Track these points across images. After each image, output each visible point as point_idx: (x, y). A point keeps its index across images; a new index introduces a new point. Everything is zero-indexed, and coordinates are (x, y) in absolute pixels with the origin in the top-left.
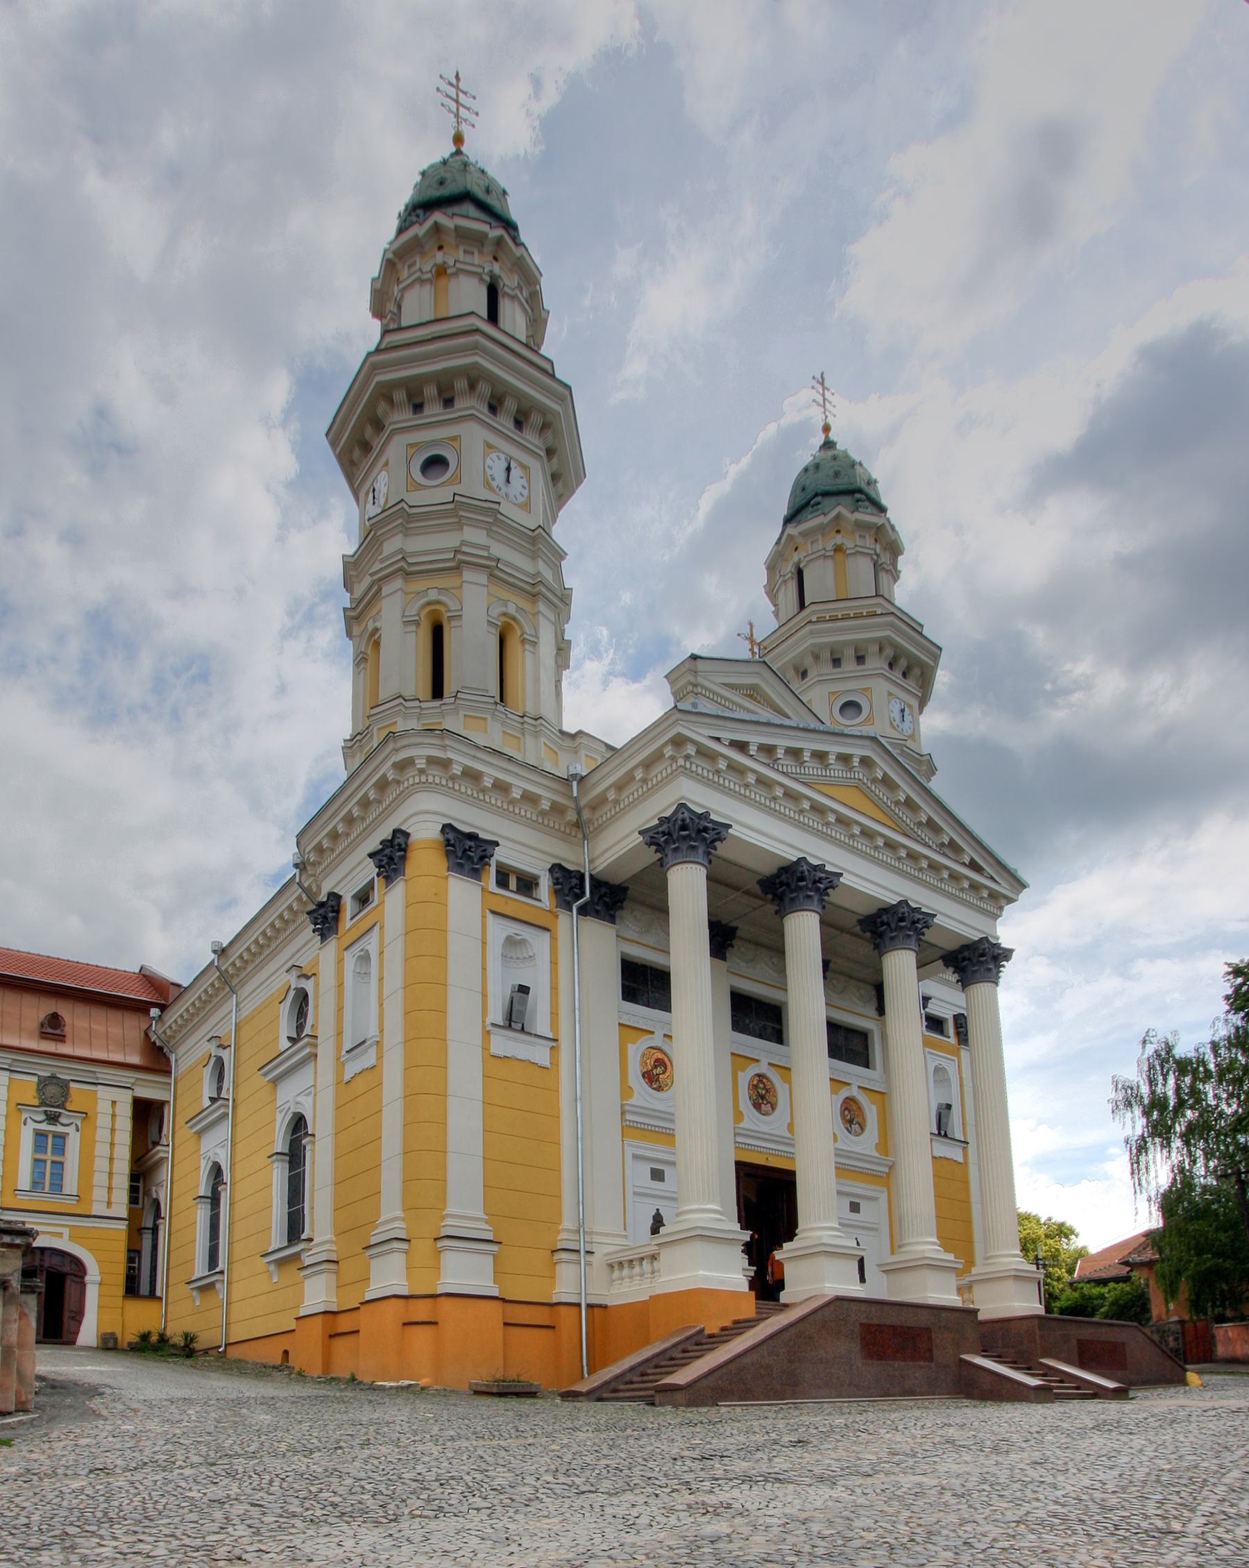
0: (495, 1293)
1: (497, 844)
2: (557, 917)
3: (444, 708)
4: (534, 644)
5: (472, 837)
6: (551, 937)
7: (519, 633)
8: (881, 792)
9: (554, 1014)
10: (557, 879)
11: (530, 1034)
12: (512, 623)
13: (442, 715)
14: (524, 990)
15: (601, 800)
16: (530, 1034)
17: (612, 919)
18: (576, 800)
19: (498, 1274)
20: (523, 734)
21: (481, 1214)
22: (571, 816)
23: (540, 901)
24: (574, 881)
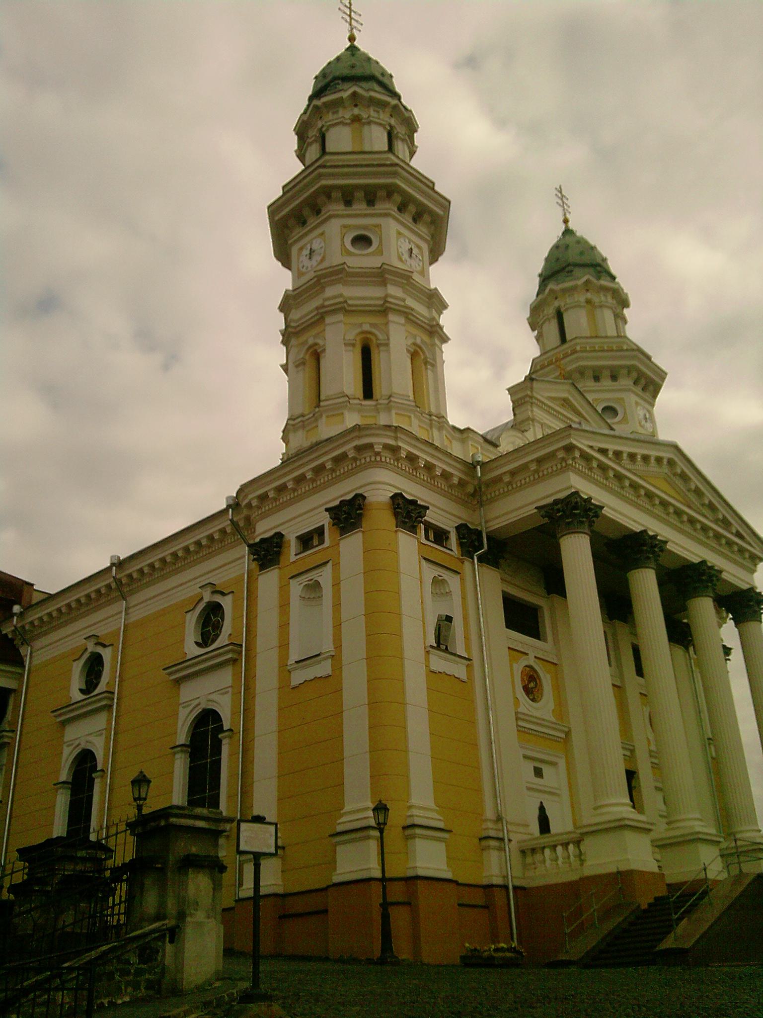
0: (449, 875)
1: (428, 508)
2: (463, 563)
3: (379, 406)
4: (433, 365)
6: (462, 580)
7: (422, 358)
8: (679, 482)
9: (467, 638)
10: (464, 535)
11: (454, 655)
12: (419, 350)
13: (378, 411)
14: (449, 619)
15: (498, 480)
16: (454, 655)
17: (498, 568)
18: (480, 479)
19: (451, 859)
20: (431, 428)
21: (432, 805)
22: (470, 489)
23: (452, 550)
24: (474, 537)
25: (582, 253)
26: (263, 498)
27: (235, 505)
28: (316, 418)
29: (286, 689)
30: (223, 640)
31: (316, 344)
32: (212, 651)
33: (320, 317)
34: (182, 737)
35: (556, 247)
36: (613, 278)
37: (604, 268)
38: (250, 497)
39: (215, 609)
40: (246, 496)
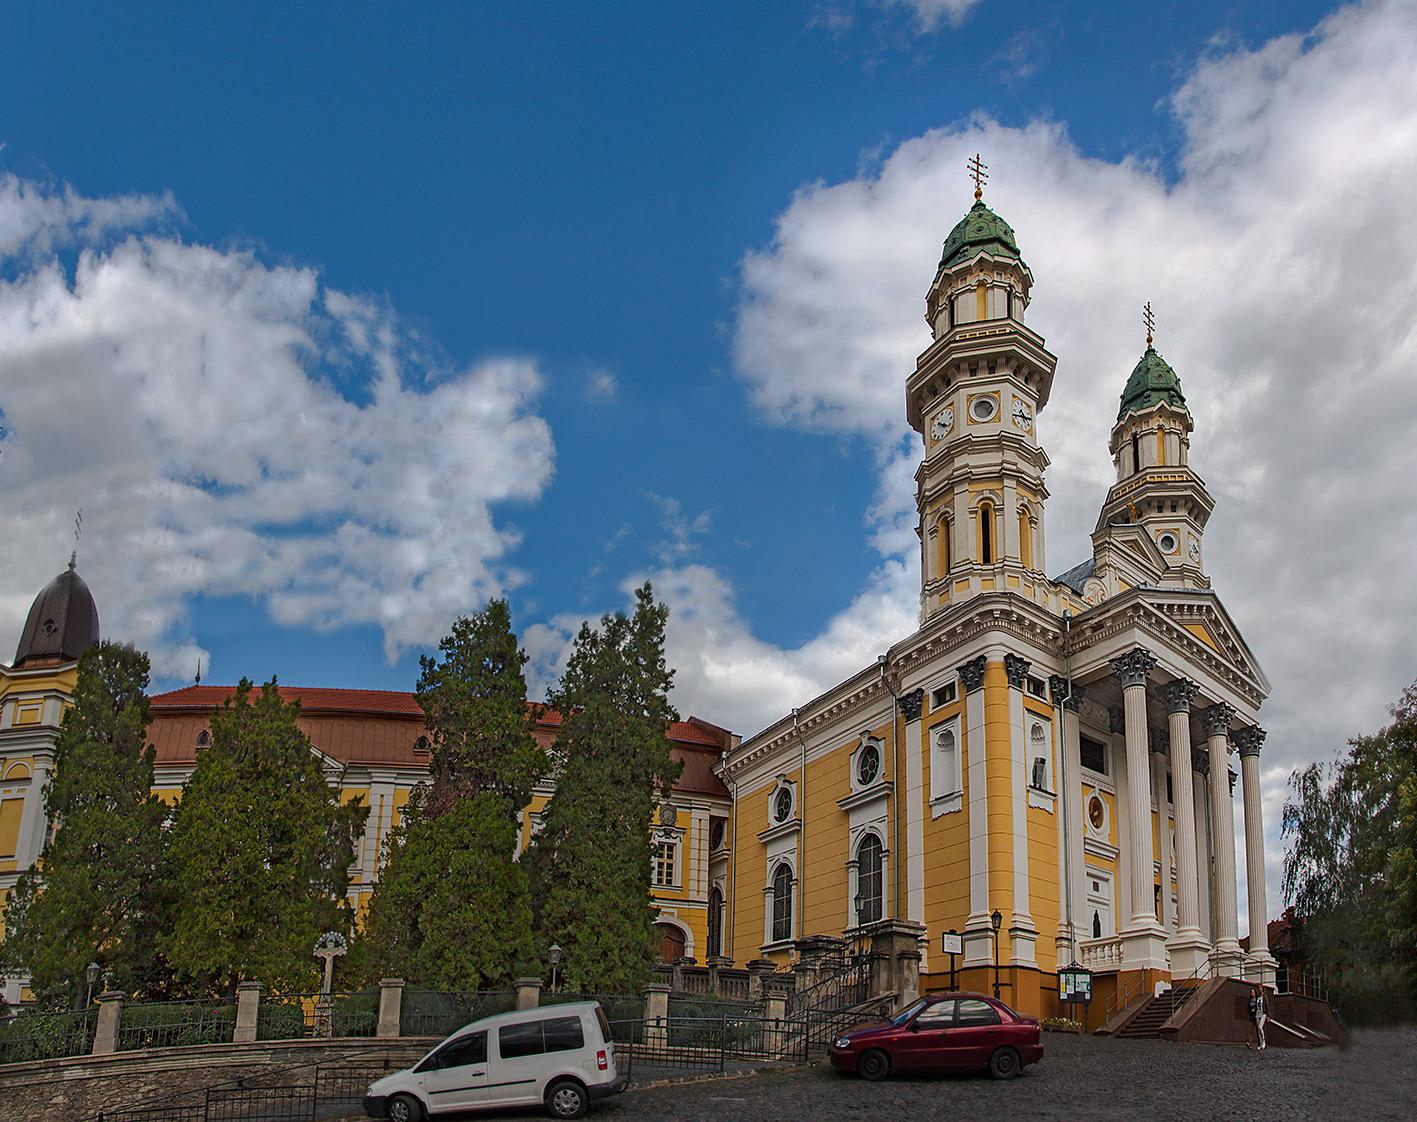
5: (1021, 660)
25: (1160, 376)
26: (908, 658)
27: (885, 663)
28: (948, 584)
29: (930, 821)
30: (878, 780)
31: (947, 512)
32: (870, 789)
33: (949, 489)
34: (853, 857)
35: (1138, 369)
36: (1183, 400)
37: (1176, 392)
38: (898, 657)
39: (870, 753)
40: (895, 656)
